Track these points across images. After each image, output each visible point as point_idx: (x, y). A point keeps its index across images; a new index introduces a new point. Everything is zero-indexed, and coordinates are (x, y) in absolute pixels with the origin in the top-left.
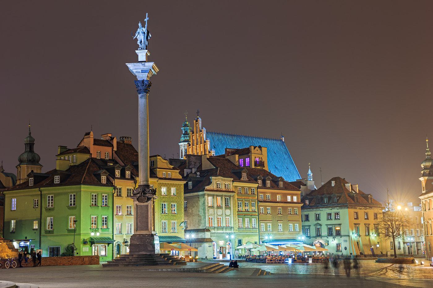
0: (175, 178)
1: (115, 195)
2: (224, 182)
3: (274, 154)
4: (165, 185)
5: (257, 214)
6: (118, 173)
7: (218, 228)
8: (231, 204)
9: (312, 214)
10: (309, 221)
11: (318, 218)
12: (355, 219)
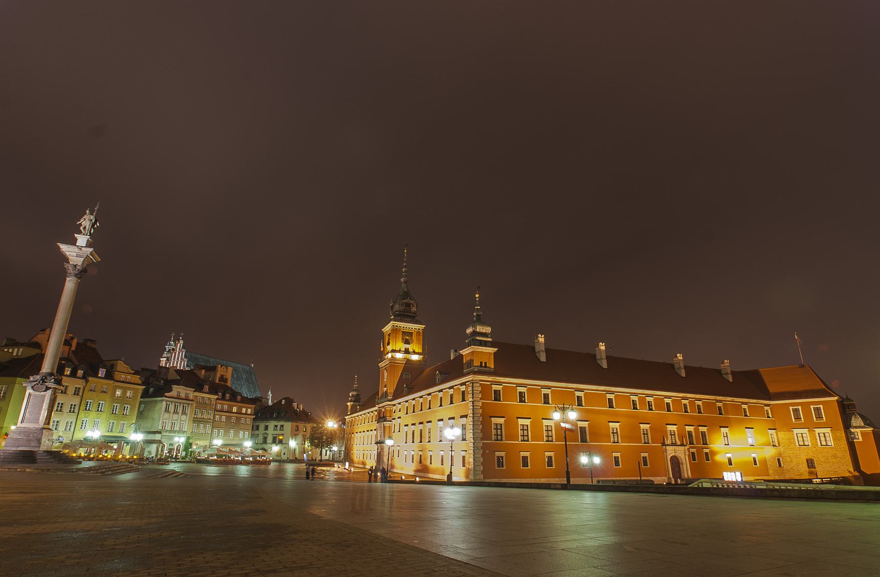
4: (120, 388)
7: (170, 431)
8: (188, 411)
9: (262, 426)
11: (266, 428)
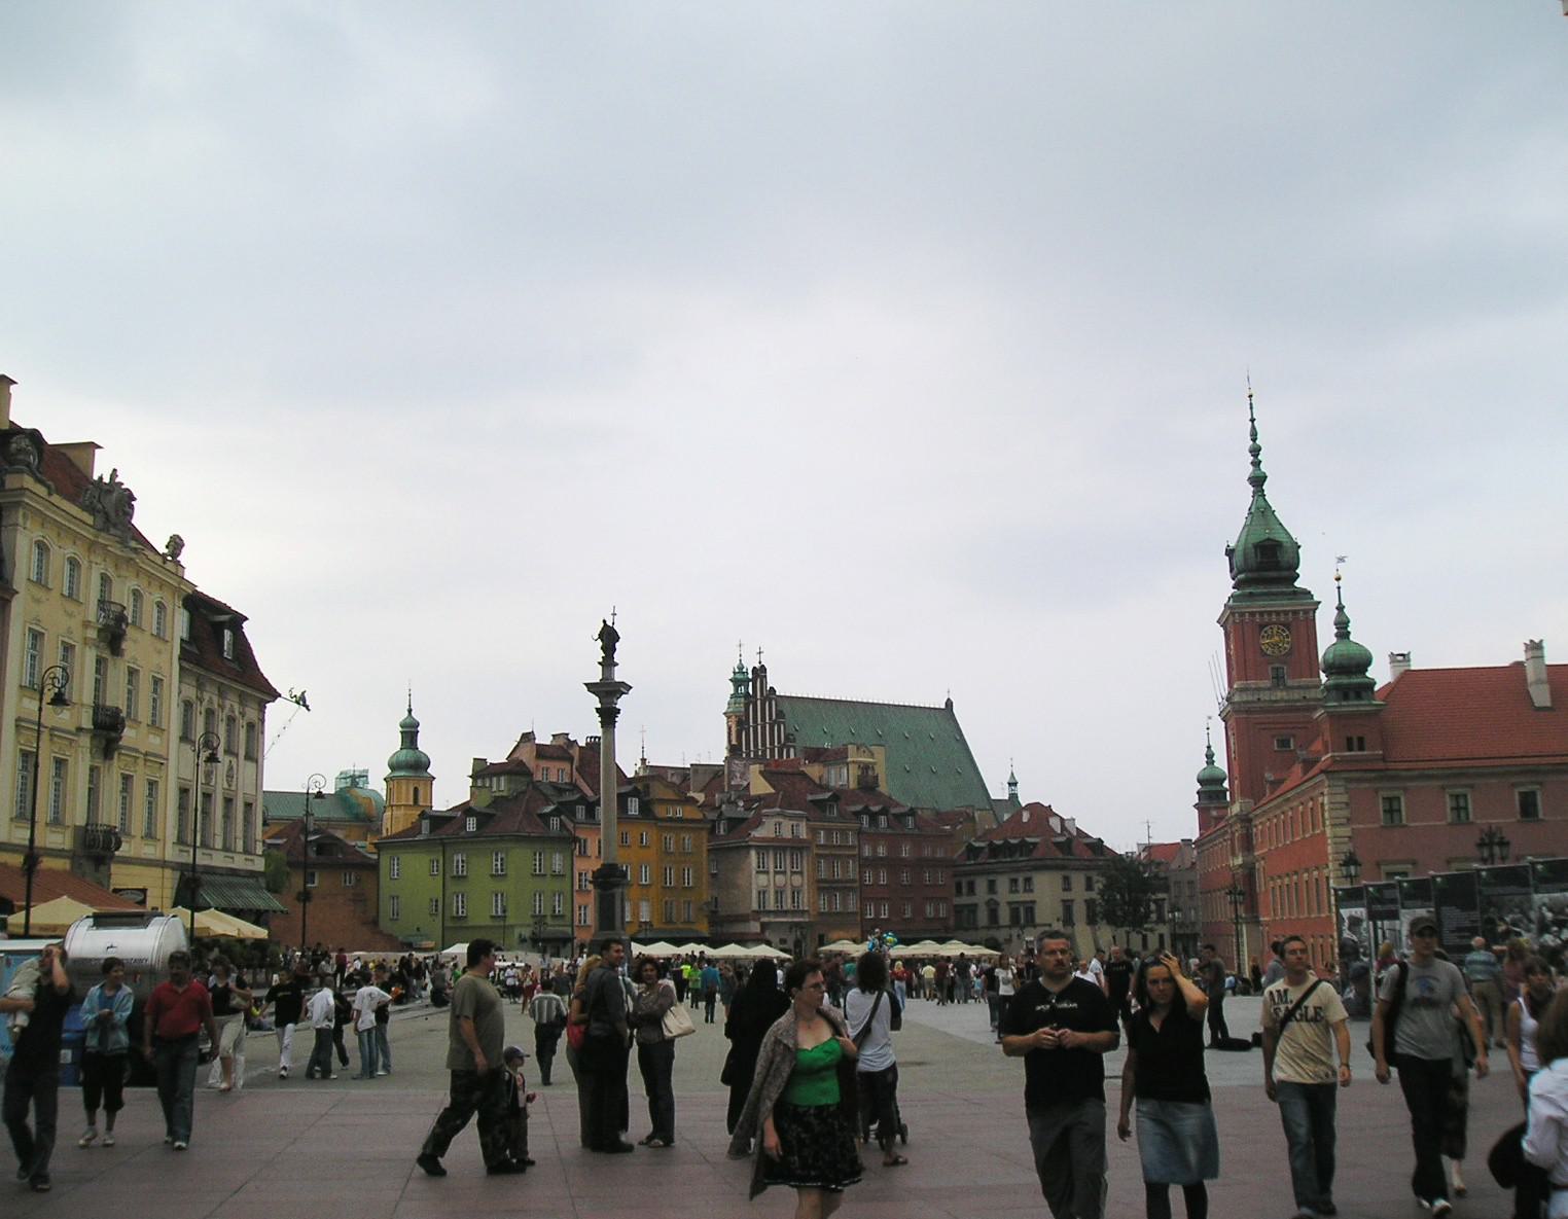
0: (690, 817)
1: (577, 852)
2: (792, 822)
3: (929, 740)
5: (857, 885)
10: (975, 894)
12: (1065, 890)
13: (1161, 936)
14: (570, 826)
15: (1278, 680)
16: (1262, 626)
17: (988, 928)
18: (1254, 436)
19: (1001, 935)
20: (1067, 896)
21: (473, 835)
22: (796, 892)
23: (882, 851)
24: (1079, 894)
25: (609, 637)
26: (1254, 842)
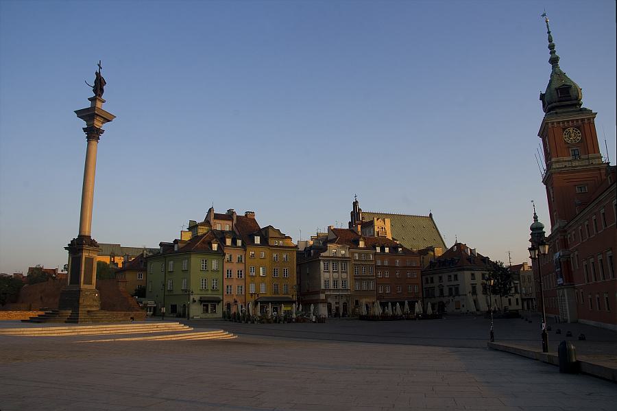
6: (229, 242)
13: (517, 300)
14: (222, 247)
15: (576, 156)
16: (564, 129)
17: (439, 297)
18: (550, 40)
19: (445, 300)
20: (473, 282)
21: (176, 252)
22: (344, 282)
23: (386, 263)
24: (479, 280)
25: (99, 85)
26: (569, 243)
